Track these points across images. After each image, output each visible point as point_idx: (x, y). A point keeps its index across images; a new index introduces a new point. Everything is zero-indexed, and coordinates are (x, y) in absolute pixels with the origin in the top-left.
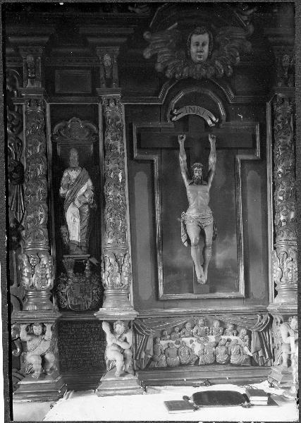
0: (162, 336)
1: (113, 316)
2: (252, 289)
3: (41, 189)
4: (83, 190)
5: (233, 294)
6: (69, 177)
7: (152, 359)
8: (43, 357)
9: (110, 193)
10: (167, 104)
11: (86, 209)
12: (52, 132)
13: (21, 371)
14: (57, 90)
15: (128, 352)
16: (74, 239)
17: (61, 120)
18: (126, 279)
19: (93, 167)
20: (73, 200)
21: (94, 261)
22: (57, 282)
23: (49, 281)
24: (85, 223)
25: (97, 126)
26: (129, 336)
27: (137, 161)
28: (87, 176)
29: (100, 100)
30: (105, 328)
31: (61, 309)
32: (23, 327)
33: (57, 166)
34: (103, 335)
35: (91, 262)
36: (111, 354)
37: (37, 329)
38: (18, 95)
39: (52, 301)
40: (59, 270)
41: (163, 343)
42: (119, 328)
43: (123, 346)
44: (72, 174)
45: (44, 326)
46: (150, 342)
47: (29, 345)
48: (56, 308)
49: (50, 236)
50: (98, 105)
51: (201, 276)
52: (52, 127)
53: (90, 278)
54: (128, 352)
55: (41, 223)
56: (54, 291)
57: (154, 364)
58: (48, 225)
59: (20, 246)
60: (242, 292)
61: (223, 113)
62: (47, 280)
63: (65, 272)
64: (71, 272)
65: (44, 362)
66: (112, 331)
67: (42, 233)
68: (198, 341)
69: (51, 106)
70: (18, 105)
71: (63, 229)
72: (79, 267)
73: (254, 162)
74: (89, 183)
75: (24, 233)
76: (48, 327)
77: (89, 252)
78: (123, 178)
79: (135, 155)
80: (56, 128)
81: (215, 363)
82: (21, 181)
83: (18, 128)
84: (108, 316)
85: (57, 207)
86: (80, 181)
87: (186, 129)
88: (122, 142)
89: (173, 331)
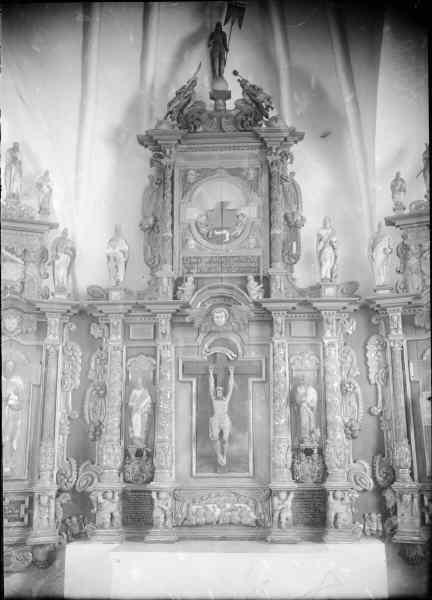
0: (194, 502)
2: (258, 471)
5: (247, 474)
6: (136, 396)
7: (185, 519)
9: (162, 406)
10: (203, 342)
11: (146, 415)
14: (131, 337)
15: (168, 513)
17: (133, 356)
19: (152, 384)
21: (150, 450)
22: (124, 463)
27: (181, 382)
28: (147, 394)
30: (154, 495)
31: (125, 481)
32: (100, 494)
33: (129, 386)
34: (152, 500)
35: (147, 451)
36: (157, 513)
37: (110, 495)
40: (126, 454)
41: (194, 508)
43: (166, 508)
44: (137, 393)
45: (113, 492)
46: (185, 504)
47: (104, 505)
51: (223, 460)
52: (127, 361)
54: (168, 513)
56: (122, 470)
57: (186, 522)
58: (120, 426)
60: (251, 474)
61: (240, 351)
63: (130, 457)
64: (133, 456)
66: (158, 496)
68: (219, 507)
71: (130, 429)
72: (139, 454)
73: (263, 382)
74: (149, 397)
75: (104, 430)
77: (146, 444)
78: (171, 396)
79: (181, 378)
80: (130, 360)
81: (231, 524)
85: (126, 411)
86: (143, 398)
87: (214, 362)
88: (171, 373)
89: (202, 499)
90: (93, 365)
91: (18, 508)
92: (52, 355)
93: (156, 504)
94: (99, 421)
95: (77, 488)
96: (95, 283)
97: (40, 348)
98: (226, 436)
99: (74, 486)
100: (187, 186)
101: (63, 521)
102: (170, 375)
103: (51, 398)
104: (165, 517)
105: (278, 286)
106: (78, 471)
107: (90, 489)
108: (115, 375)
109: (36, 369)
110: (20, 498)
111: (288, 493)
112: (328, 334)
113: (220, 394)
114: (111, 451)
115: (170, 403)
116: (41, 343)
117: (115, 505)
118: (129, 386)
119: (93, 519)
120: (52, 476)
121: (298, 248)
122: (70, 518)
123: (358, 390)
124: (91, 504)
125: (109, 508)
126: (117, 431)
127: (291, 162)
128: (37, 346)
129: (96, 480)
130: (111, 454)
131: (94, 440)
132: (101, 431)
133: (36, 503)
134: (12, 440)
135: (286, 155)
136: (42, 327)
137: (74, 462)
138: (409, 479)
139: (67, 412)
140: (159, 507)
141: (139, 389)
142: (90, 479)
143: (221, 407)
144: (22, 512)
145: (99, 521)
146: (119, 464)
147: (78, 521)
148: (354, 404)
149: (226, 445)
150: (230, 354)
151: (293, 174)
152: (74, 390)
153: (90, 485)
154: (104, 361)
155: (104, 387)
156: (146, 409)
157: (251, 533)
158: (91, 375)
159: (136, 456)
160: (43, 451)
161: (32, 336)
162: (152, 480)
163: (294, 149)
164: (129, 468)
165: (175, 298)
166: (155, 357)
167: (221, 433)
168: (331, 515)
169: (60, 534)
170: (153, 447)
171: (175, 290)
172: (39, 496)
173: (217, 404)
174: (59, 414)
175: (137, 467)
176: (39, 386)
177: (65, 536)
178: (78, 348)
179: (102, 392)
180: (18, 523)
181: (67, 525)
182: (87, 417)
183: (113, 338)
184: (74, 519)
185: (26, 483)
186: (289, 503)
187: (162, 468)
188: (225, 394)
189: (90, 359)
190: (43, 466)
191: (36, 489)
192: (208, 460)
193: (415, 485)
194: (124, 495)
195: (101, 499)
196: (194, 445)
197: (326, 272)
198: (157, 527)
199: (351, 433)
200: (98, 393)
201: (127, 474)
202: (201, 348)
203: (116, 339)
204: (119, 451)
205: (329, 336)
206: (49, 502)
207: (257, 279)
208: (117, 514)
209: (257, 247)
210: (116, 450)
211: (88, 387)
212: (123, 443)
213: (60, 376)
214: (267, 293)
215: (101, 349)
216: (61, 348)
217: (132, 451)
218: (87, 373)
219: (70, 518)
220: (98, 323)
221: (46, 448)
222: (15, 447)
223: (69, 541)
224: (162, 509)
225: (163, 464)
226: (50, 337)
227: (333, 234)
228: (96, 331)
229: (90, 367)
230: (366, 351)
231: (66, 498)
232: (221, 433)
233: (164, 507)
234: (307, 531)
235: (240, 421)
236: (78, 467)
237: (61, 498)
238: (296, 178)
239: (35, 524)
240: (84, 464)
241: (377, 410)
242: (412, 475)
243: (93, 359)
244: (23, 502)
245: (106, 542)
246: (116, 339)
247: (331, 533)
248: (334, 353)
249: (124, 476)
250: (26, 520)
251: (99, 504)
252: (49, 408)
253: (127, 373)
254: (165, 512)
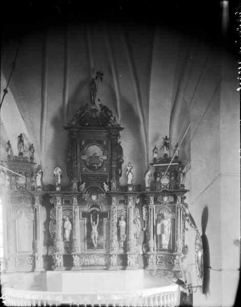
30: (73, 256)
37: (59, 256)
41: (86, 260)
51: (95, 245)
85: (64, 230)
98: (96, 238)
100: (82, 148)
102: (78, 217)
105: (114, 185)
107: (52, 255)
111: (115, 255)
112: (130, 203)
113: (94, 223)
119: (54, 264)
121: (121, 171)
123: (139, 222)
127: (120, 138)
135: (118, 135)
138: (153, 251)
143: (95, 228)
145: (56, 265)
148: (138, 227)
149: (97, 241)
150: (98, 210)
151: (120, 142)
157: (105, 267)
163: (120, 133)
165: (79, 190)
167: (95, 237)
168: (128, 262)
171: (78, 187)
173: (93, 227)
183: (58, 204)
186: (116, 258)
188: (96, 223)
192: (90, 245)
193: (155, 252)
196: (86, 240)
197: (129, 182)
199: (135, 235)
202: (87, 209)
205: (130, 203)
207: (106, 183)
209: (107, 171)
214: (110, 188)
227: (132, 168)
230: (142, 209)
232: (95, 237)
234: (121, 267)
235: (100, 232)
238: (121, 144)
241: (144, 229)
242: (154, 250)
247: (128, 267)
248: (132, 211)
251: (56, 260)
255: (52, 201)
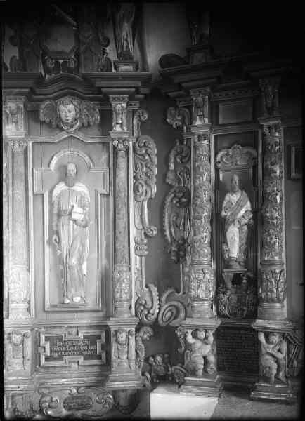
1: (269, 328)
3: (206, 213)
4: (242, 212)
6: (230, 202)
8: (205, 358)
11: (245, 228)
12: (215, 159)
13: (184, 366)
14: (221, 122)
15: (283, 362)
16: (233, 256)
18: (282, 294)
20: (233, 221)
22: (217, 292)
23: (211, 293)
24: (244, 242)
25: (257, 151)
26: (284, 346)
28: (247, 199)
29: (262, 127)
30: (262, 338)
31: (219, 315)
32: (190, 332)
34: (259, 343)
35: (248, 277)
37: (202, 335)
38: (187, 131)
39: (212, 308)
40: (220, 281)
42: (276, 338)
43: (280, 356)
44: (233, 198)
45: (206, 331)
48: (216, 314)
49: (212, 254)
50: (257, 132)
52: (216, 154)
53: (246, 291)
55: (206, 242)
56: (216, 301)
59: (186, 260)
62: (210, 291)
64: (230, 285)
65: (206, 362)
67: (206, 251)
69: (215, 137)
70: (188, 139)
71: (225, 248)
72: (237, 279)
74: (249, 204)
75: (189, 248)
76: (211, 334)
78: (281, 198)
82: (188, 204)
83: (187, 159)
84: (264, 328)
85: (220, 225)
86: (240, 205)
88: (281, 166)
90: (172, 166)
91: (94, 343)
92: (122, 153)
93: (263, 351)
94: (184, 239)
95: (161, 322)
96: (163, 53)
97: (105, 145)
99: (157, 319)
101: (146, 360)
103: (124, 211)
104: (279, 370)
106: (159, 300)
107: (174, 323)
108: (202, 175)
109: (101, 171)
110: (96, 332)
114: (201, 276)
115: (280, 209)
116: (106, 139)
117: (209, 347)
118: (220, 189)
120: (130, 307)
122: (154, 357)
124: (179, 342)
125: (203, 350)
126: (207, 251)
128: (103, 143)
129: (182, 315)
130: (202, 282)
131: (178, 262)
132: (185, 251)
133: (113, 339)
134: (80, 264)
136: (106, 121)
137: (154, 290)
139: (144, 228)
140: (268, 353)
141: (234, 192)
142: (175, 311)
144: (99, 350)
146: (212, 293)
147: (163, 360)
152: (151, 198)
153: (176, 317)
154: (185, 158)
155: (187, 194)
156: (245, 221)
158: (170, 179)
159: (233, 283)
160: (118, 276)
161: (96, 131)
162: (254, 315)
164: (225, 299)
166: (256, 148)
169: (143, 374)
170: (256, 272)
172: (116, 332)
174: (133, 232)
175: (234, 297)
176: (108, 195)
177: (149, 376)
178: (152, 145)
179: (186, 200)
180: (95, 362)
181: (150, 365)
182: (167, 233)
184: (159, 358)
185: (101, 314)
187: (273, 300)
189: (167, 161)
190: (118, 295)
191: (112, 323)
194: (221, 333)
195: (190, 339)
198: (267, 380)
200: (179, 202)
201: (222, 307)
203: (201, 123)
204: (210, 276)
206: (128, 339)
208: (212, 359)
210: (208, 276)
211: (166, 195)
212: (214, 266)
213: (132, 181)
215: (182, 142)
216: (131, 144)
217: (228, 275)
218: (165, 176)
219: (154, 357)
220: (176, 107)
221: (119, 272)
222: (85, 272)
223: (154, 386)
224: (273, 356)
225: (274, 296)
226: (118, 128)
228: (174, 121)
229: (168, 166)
231: (147, 333)
233: (274, 352)
236: (160, 295)
237: (142, 332)
239: (114, 365)
240: (167, 293)
243: (172, 156)
244: (99, 337)
245: (198, 394)
246: (201, 123)
249: (217, 307)
250: (104, 355)
251: (188, 346)
252: (121, 224)
253: (217, 171)
254: (277, 361)
255: (174, 121)
